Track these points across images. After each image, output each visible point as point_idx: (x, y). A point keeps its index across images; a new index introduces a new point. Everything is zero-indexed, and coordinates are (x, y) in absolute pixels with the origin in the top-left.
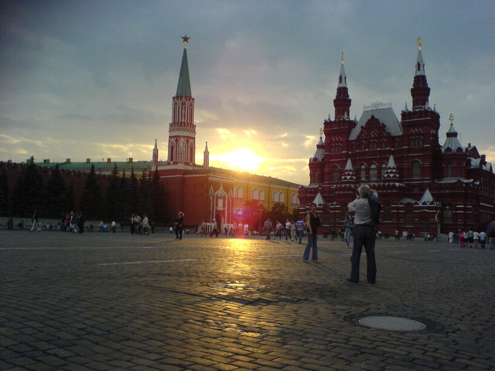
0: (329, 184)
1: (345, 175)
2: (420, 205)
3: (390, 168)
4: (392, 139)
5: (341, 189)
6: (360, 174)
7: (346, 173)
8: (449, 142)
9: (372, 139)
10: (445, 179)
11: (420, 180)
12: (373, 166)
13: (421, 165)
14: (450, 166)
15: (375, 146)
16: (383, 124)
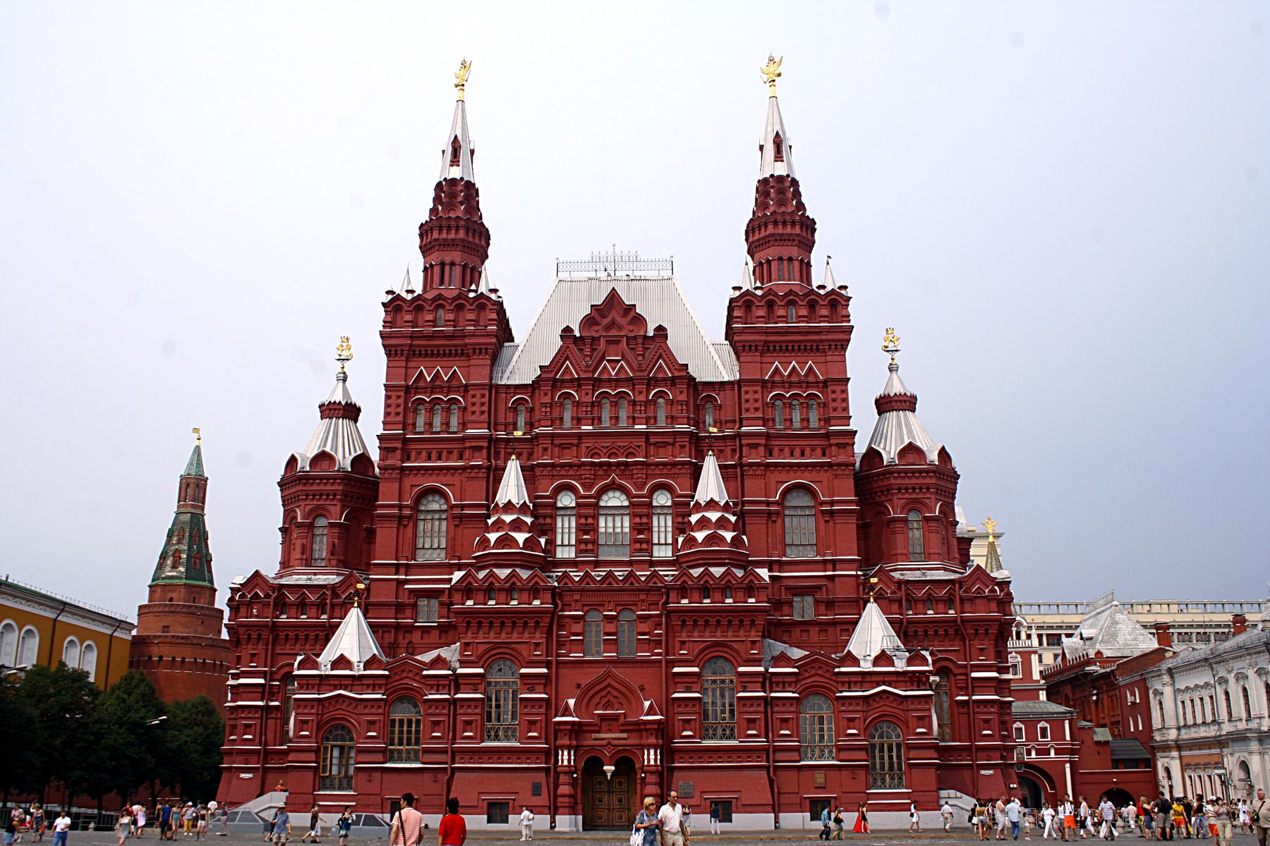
0: (397, 568)
1: (499, 525)
2: (866, 666)
3: (712, 505)
4: (699, 394)
5: (489, 589)
6: (549, 531)
7: (508, 518)
8: (899, 425)
9: (617, 382)
10: (900, 565)
11: (824, 564)
12: (614, 499)
13: (822, 503)
14: (913, 516)
15: (623, 415)
16: (661, 330)
